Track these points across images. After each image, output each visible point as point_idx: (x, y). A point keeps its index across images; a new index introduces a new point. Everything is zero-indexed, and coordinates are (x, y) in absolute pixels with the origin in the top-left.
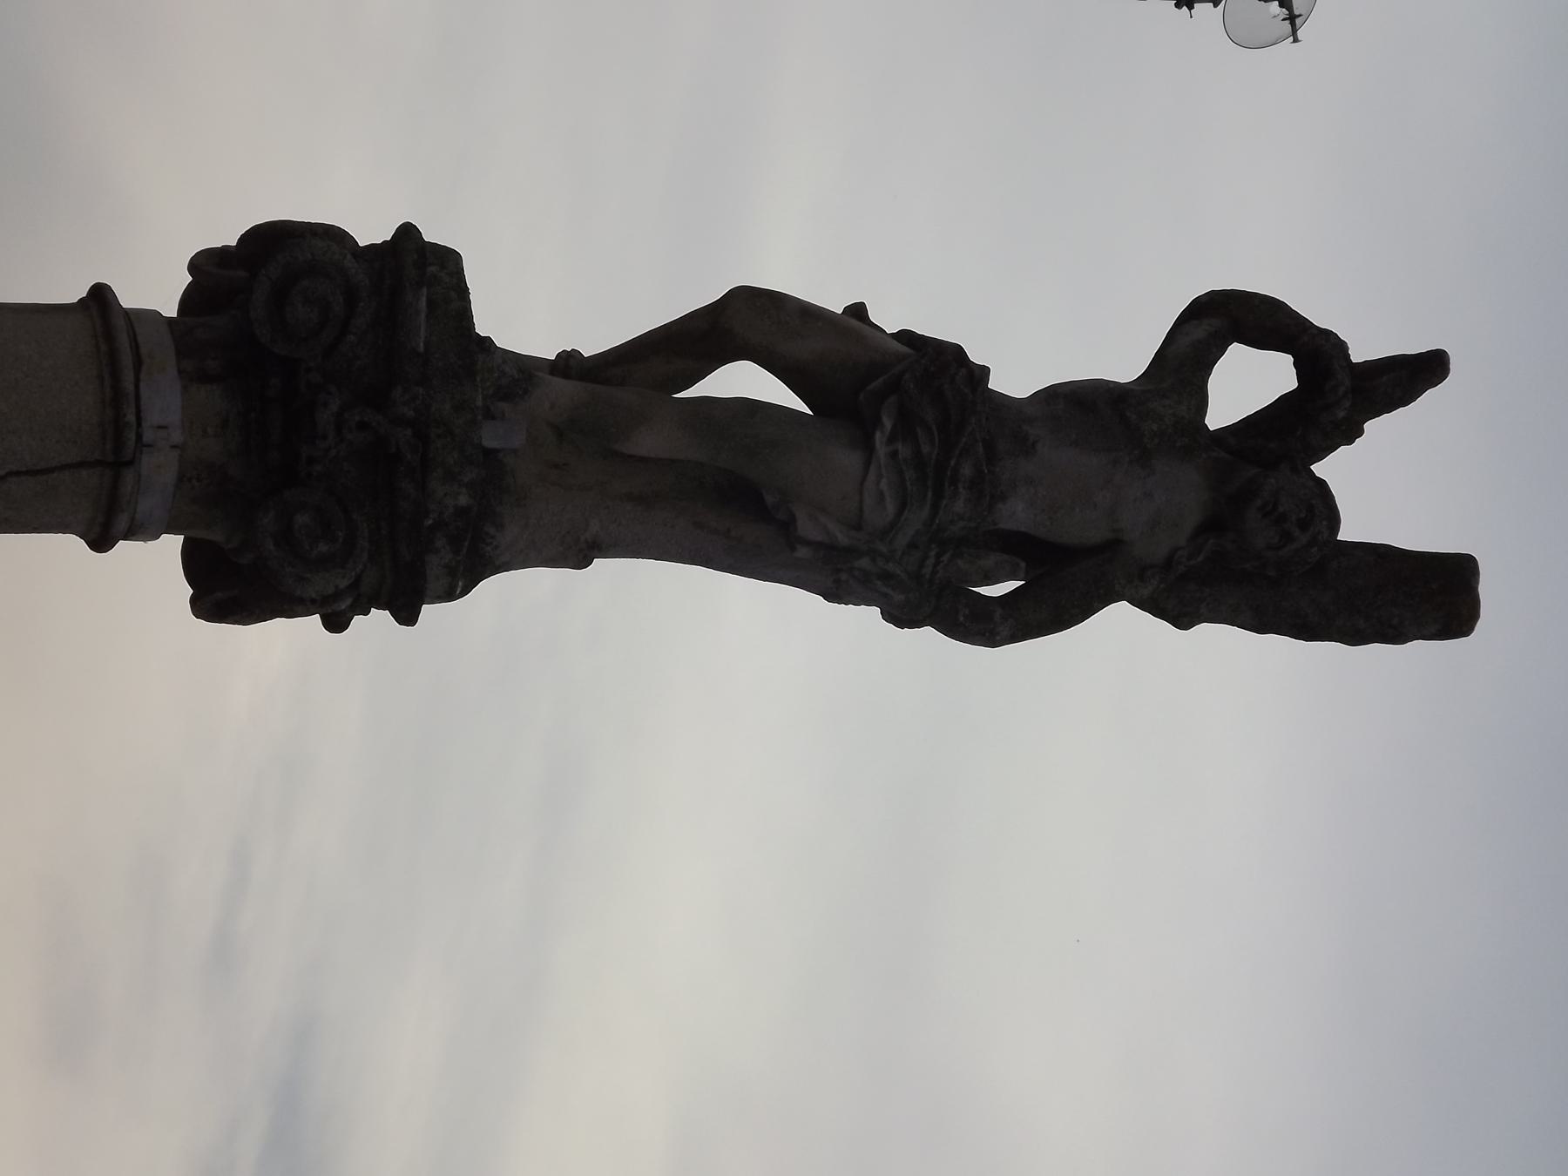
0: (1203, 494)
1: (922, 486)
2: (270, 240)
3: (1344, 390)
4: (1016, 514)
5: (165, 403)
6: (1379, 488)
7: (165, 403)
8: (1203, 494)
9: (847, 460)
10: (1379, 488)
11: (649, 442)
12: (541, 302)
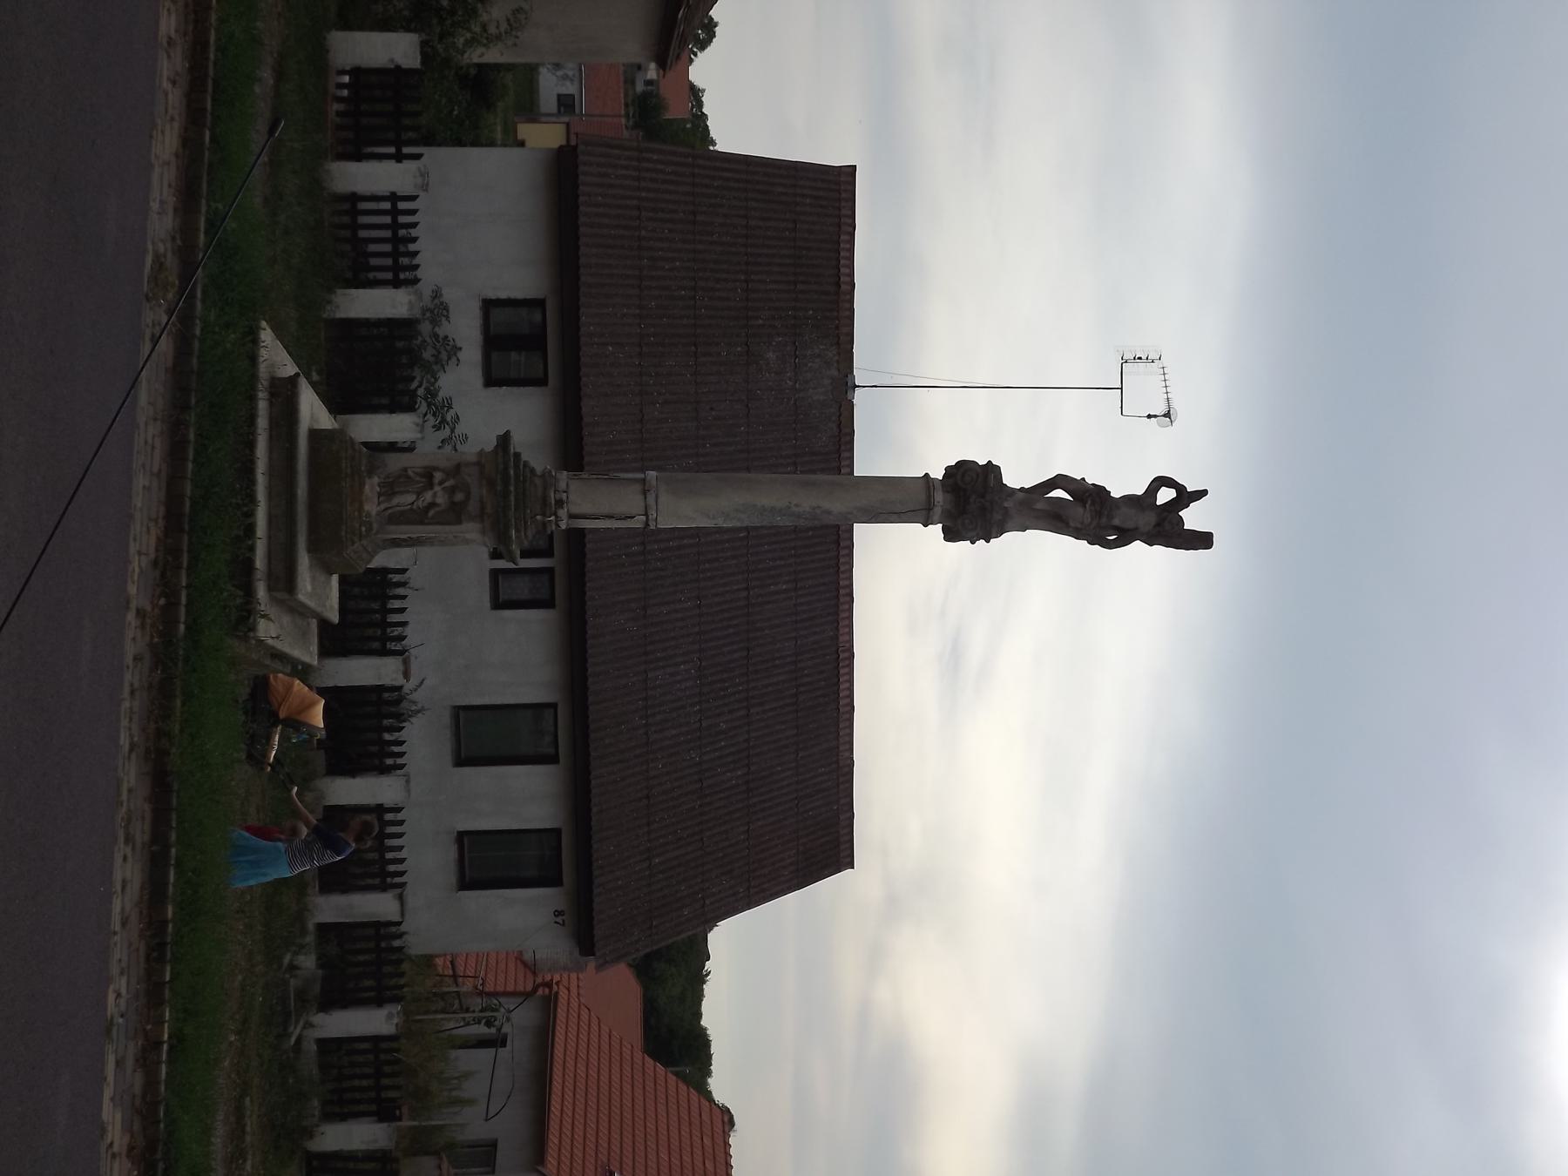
0: (1157, 519)
1: (1092, 514)
2: (961, 464)
3: (1186, 497)
4: (1116, 522)
5: (939, 497)
6: (1192, 517)
7: (939, 497)
8: (1157, 519)
9: (1080, 510)
10: (1192, 517)
11: (1039, 506)
12: (1016, 477)
